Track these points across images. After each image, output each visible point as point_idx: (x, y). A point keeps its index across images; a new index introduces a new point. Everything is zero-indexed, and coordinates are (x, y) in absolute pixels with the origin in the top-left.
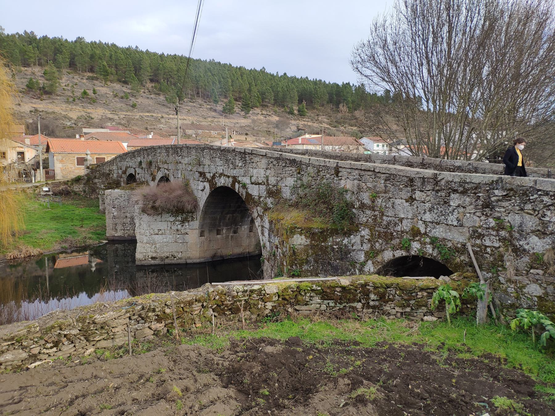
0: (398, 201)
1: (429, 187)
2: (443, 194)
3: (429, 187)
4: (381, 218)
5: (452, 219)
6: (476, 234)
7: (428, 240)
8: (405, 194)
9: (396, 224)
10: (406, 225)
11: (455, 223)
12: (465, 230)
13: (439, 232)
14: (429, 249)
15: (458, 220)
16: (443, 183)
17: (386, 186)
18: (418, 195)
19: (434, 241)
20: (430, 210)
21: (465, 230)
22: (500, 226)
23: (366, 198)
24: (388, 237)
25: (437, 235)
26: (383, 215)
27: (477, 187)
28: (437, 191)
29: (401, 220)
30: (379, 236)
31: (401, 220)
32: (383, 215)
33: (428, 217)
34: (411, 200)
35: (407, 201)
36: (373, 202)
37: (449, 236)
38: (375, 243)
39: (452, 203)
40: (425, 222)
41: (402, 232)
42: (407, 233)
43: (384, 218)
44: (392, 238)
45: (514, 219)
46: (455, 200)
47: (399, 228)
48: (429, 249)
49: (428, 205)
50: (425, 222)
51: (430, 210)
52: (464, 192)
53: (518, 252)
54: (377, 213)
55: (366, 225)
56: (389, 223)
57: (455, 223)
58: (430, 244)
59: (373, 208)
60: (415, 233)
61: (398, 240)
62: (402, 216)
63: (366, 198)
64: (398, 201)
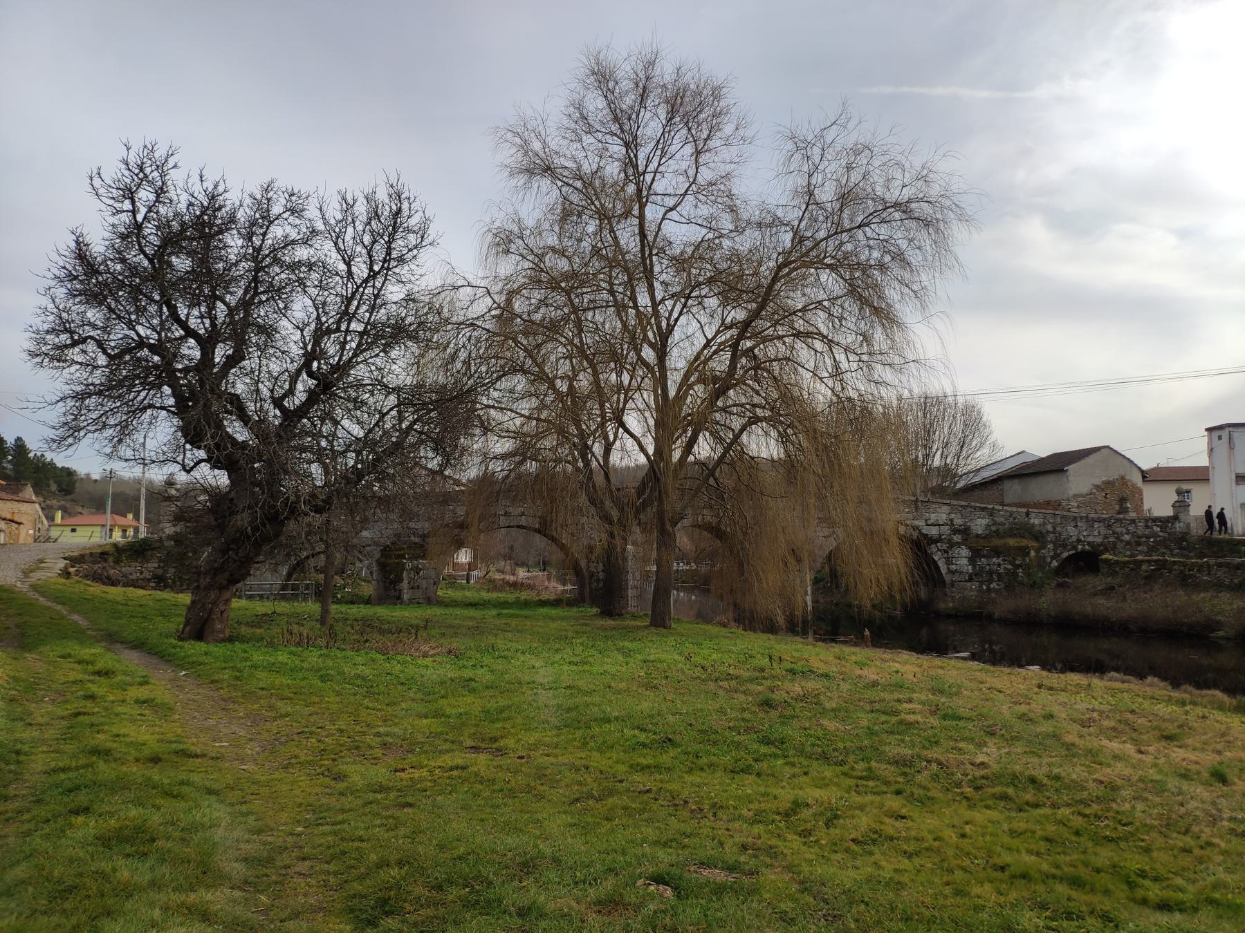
5: (1096, 533)
6: (1106, 537)
10: (1074, 539)
13: (1090, 539)
14: (1087, 547)
19: (1089, 544)
22: (1114, 533)
23: (1050, 528)
24: (1064, 546)
27: (1105, 519)
33: (1085, 533)
34: (1076, 526)
45: (1119, 530)
48: (1087, 547)
53: (1122, 541)
55: (1051, 542)
59: (1054, 533)
60: (1079, 541)
63: (1050, 528)
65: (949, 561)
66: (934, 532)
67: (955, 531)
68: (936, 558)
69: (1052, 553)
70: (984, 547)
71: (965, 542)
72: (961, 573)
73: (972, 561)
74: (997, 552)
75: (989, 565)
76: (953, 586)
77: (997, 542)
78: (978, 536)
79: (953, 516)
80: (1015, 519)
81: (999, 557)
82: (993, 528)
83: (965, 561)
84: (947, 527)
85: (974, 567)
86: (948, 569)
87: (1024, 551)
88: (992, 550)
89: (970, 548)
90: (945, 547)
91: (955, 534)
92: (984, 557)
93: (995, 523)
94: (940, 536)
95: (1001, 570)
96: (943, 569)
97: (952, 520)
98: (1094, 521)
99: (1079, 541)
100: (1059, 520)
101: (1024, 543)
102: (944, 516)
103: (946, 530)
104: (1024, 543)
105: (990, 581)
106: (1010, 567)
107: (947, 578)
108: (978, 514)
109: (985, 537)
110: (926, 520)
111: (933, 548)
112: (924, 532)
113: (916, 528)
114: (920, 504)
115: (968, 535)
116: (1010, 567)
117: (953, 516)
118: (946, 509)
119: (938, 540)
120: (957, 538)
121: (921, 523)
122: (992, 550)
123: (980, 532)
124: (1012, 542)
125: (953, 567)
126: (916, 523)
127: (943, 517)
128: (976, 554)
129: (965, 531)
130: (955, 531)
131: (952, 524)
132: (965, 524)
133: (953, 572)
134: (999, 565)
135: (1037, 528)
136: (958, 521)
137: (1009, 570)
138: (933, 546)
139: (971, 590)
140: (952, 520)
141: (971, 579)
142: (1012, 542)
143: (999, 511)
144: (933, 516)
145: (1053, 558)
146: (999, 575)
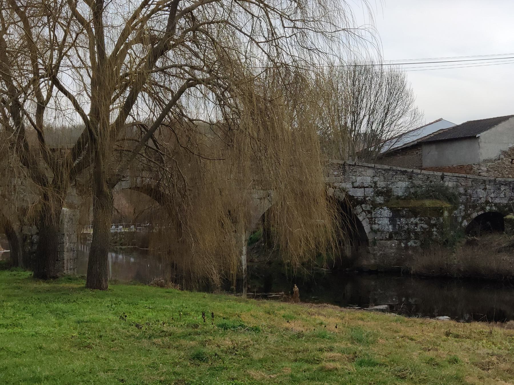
0: (479, 190)
1: (492, 184)
2: (498, 186)
3: (492, 184)
4: (471, 199)
5: (502, 195)
7: (493, 205)
8: (482, 187)
9: (478, 200)
10: (483, 200)
11: (503, 196)
12: (507, 198)
13: (497, 201)
14: (494, 208)
15: (505, 195)
16: (497, 182)
17: (472, 184)
18: (487, 186)
19: (496, 205)
20: (494, 192)
21: (507, 198)
24: (474, 207)
25: (497, 202)
26: (471, 197)
27: (510, 182)
28: (496, 185)
29: (480, 198)
30: (470, 207)
31: (480, 198)
32: (471, 197)
33: (492, 195)
34: (485, 189)
35: (483, 190)
36: (466, 191)
37: (501, 201)
38: (467, 211)
39: (501, 189)
40: (491, 198)
41: (481, 203)
42: (483, 203)
43: (472, 198)
44: (476, 206)
46: (503, 188)
47: (480, 202)
48: (494, 208)
49: (492, 191)
50: (491, 198)
51: (494, 192)
52: (506, 185)
54: (468, 197)
56: (474, 201)
57: (503, 196)
58: (494, 206)
59: (465, 195)
60: (487, 202)
61: (479, 207)
62: (481, 196)
63: (462, 190)
64: (479, 190)
65: (372, 221)
66: (359, 194)
67: (379, 193)
68: (360, 218)
69: (463, 214)
70: (404, 208)
71: (387, 203)
72: (382, 232)
73: (392, 220)
74: (414, 212)
75: (407, 224)
76: (374, 243)
77: (414, 203)
78: (398, 198)
79: (376, 179)
80: (431, 182)
81: (416, 217)
82: (412, 191)
83: (386, 221)
84: (371, 190)
85: (394, 226)
86: (371, 228)
87: (438, 212)
88: (410, 211)
89: (391, 209)
90: (368, 208)
91: (378, 196)
92: (403, 217)
93: (414, 186)
94: (365, 197)
95: (418, 229)
96: (367, 228)
97: (375, 183)
98: (501, 184)
99: (487, 202)
100: (470, 184)
101: (438, 203)
102: (369, 179)
103: (370, 192)
104: (438, 203)
105: (408, 239)
106: (425, 226)
107: (370, 237)
108: (399, 177)
109: (406, 199)
110: (353, 183)
111: (358, 209)
112: (351, 193)
113: (343, 190)
114: (347, 168)
115: (390, 196)
116: (425, 226)
117: (376, 179)
118: (370, 172)
119: (363, 201)
120: (380, 200)
121: (348, 186)
122: (410, 211)
123: (400, 194)
124: (428, 203)
125: (376, 227)
126: (343, 185)
127: (368, 180)
128: (396, 214)
129: (387, 193)
130: (379, 193)
131: (376, 186)
132: (387, 187)
133: (375, 232)
134: (416, 225)
135: (450, 191)
136: (381, 184)
137: (425, 229)
138: (358, 207)
139: (391, 247)
140: (375, 183)
141: (391, 238)
142: (428, 203)
143: (418, 174)
144: (359, 179)
145: (464, 218)
146: (416, 234)
